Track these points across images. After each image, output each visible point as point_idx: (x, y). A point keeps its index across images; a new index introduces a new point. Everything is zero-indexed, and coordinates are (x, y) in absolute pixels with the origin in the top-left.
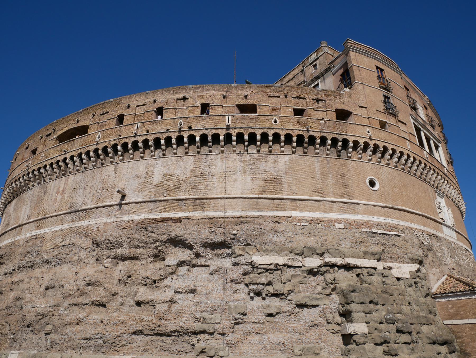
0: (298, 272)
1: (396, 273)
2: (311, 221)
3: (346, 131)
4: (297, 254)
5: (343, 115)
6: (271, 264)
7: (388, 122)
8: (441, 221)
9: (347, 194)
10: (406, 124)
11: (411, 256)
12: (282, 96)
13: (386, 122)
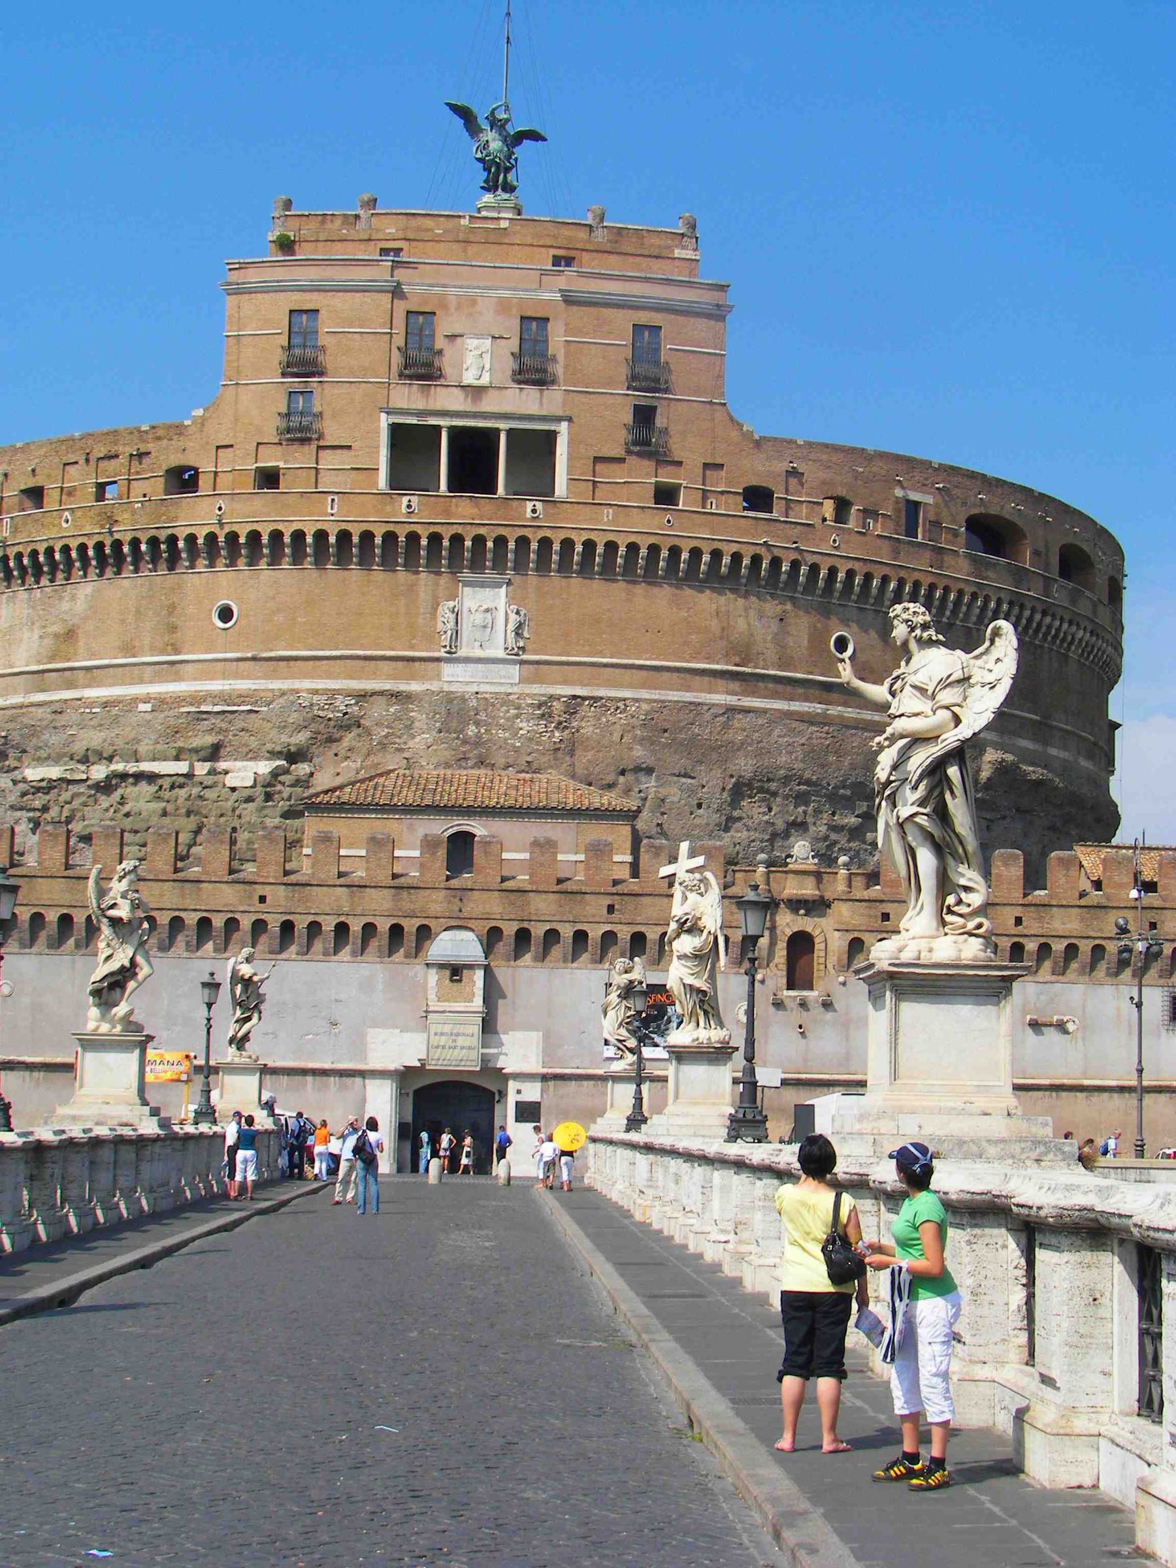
0: (82, 789)
1: (230, 781)
2: (106, 704)
3: (176, 519)
4: (79, 761)
5: (183, 480)
6: (42, 780)
7: (282, 465)
8: (442, 653)
9: (172, 645)
10: (349, 447)
11: (269, 746)
12: (82, 461)
13: (277, 468)
